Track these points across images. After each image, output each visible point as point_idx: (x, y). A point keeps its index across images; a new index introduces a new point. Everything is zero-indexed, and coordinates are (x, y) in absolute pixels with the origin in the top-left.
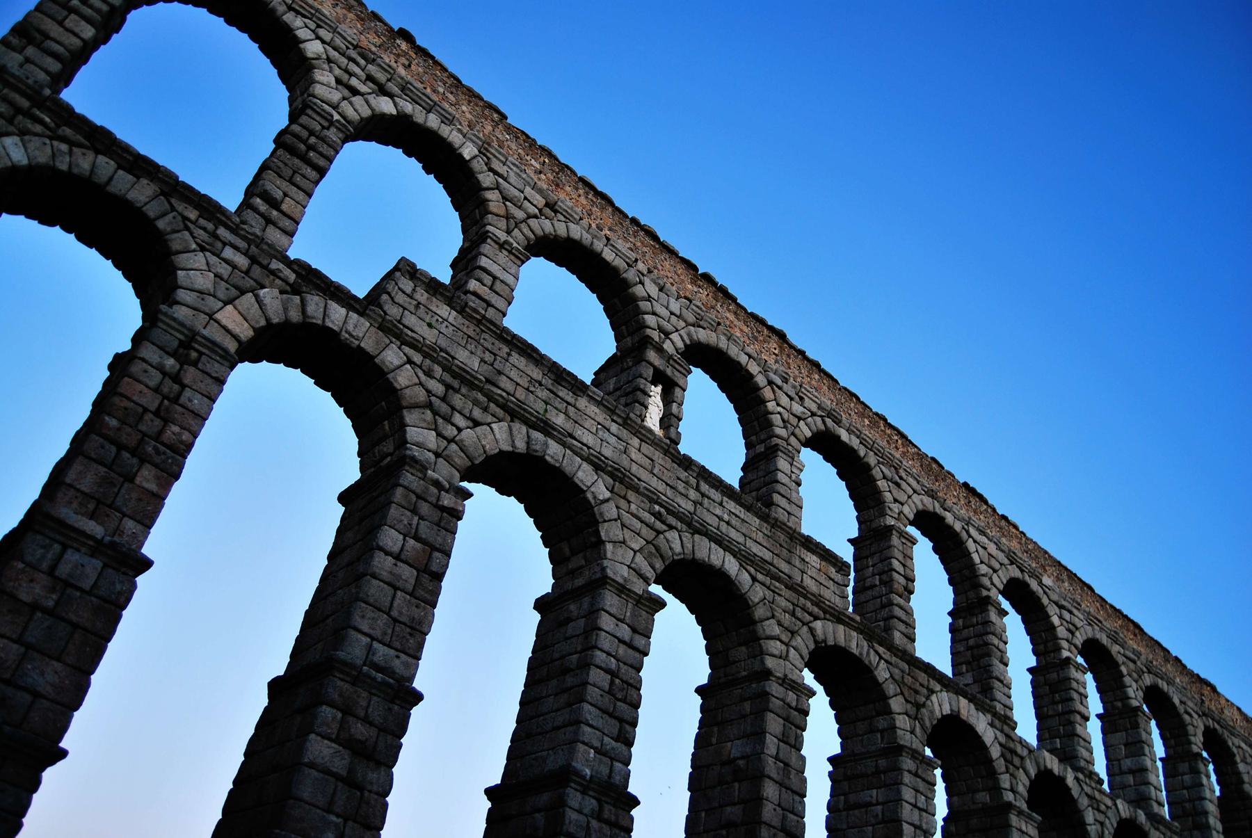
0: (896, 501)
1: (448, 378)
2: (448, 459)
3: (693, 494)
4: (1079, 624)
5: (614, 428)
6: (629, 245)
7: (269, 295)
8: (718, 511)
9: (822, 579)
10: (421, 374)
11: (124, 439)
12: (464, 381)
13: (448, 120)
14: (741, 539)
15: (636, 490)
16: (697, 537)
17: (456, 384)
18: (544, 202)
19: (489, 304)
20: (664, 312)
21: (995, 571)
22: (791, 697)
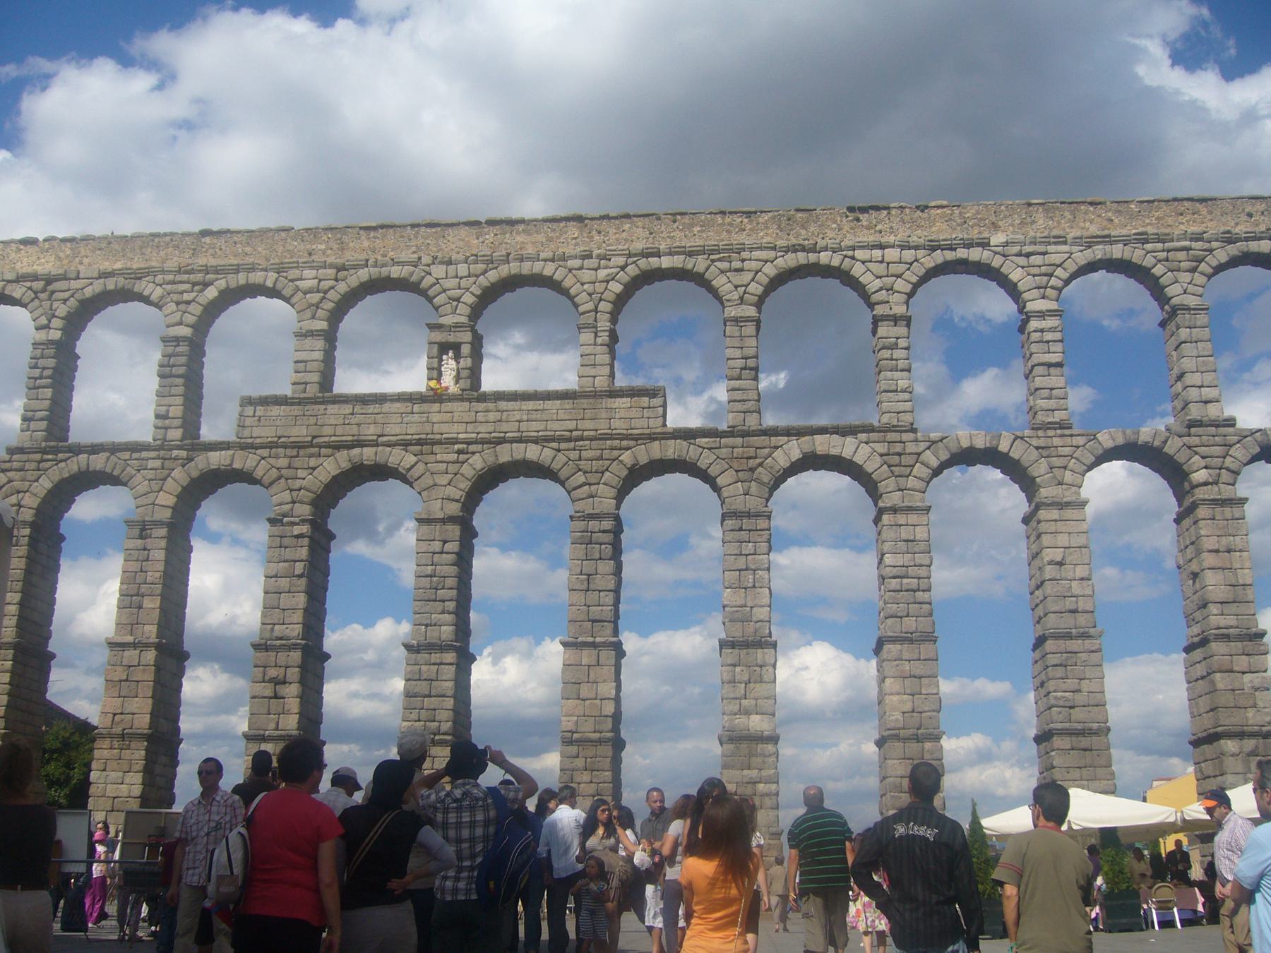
0: (736, 287)
1: (290, 452)
2: (301, 502)
3: (492, 416)
4: (1056, 259)
5: (416, 408)
6: (414, 249)
7: (178, 473)
8: (518, 417)
9: (633, 413)
10: (272, 461)
11: (132, 593)
12: (299, 448)
13: (252, 268)
14: (541, 426)
15: (440, 443)
16: (499, 448)
17: (294, 452)
18: (334, 271)
19: (306, 384)
20: (451, 283)
21: (899, 276)
22: (594, 525)
